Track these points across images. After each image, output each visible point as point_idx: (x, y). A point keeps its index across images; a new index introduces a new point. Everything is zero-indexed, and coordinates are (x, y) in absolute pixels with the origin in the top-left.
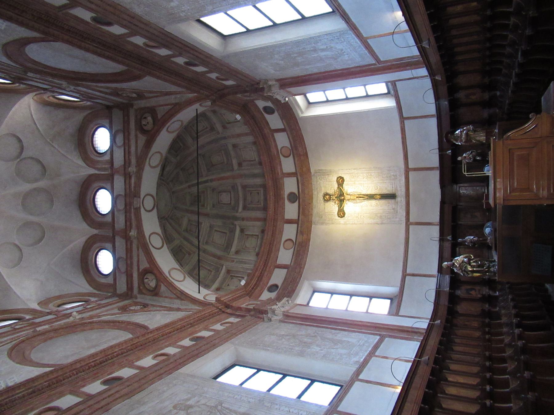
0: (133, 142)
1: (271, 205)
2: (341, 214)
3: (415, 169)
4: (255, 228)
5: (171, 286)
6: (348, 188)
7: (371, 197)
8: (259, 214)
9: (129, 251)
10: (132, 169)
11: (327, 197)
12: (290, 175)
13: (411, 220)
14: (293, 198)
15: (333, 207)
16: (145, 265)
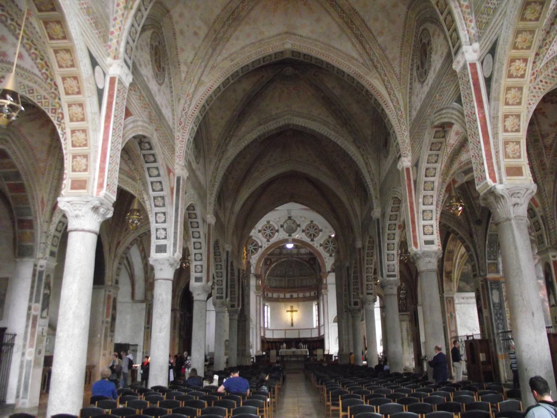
0: (306, 256)
1: (289, 290)
2: (287, 311)
3: (299, 333)
4: (283, 284)
5: (267, 269)
6: (294, 313)
7: (292, 320)
8: (287, 285)
9: (276, 255)
10: (299, 256)
11: (292, 307)
12: (298, 295)
13: (287, 331)
14: (291, 296)
15: (289, 309)
16: (273, 260)
